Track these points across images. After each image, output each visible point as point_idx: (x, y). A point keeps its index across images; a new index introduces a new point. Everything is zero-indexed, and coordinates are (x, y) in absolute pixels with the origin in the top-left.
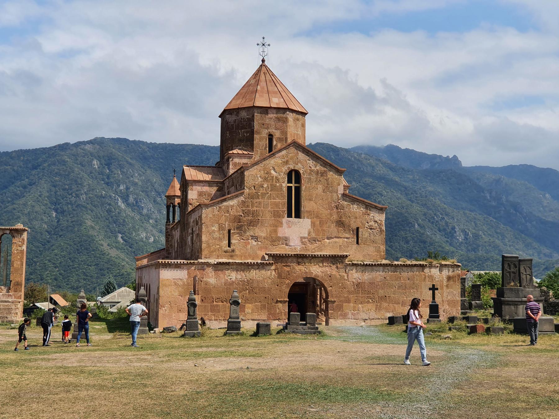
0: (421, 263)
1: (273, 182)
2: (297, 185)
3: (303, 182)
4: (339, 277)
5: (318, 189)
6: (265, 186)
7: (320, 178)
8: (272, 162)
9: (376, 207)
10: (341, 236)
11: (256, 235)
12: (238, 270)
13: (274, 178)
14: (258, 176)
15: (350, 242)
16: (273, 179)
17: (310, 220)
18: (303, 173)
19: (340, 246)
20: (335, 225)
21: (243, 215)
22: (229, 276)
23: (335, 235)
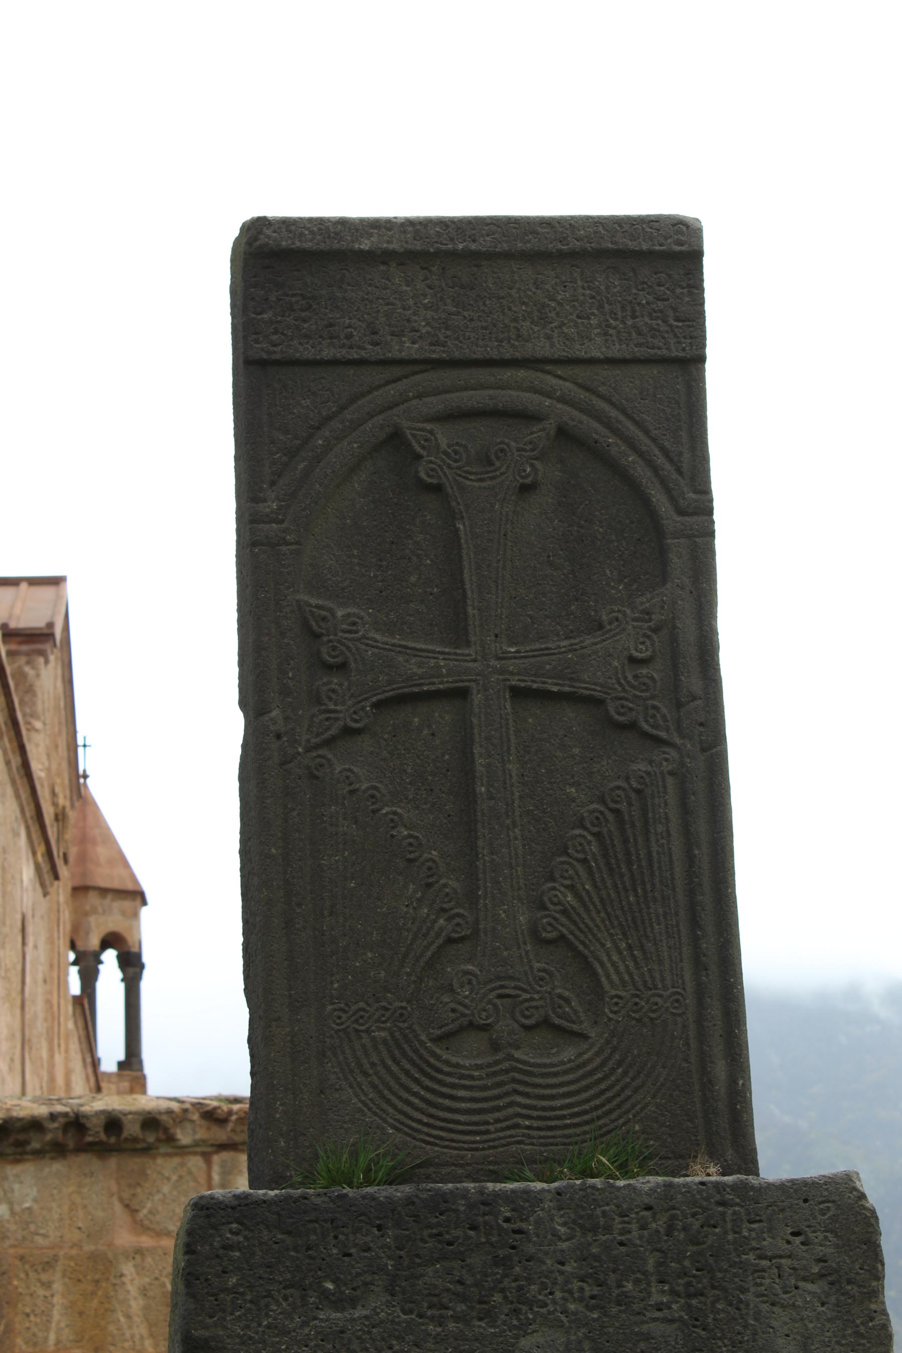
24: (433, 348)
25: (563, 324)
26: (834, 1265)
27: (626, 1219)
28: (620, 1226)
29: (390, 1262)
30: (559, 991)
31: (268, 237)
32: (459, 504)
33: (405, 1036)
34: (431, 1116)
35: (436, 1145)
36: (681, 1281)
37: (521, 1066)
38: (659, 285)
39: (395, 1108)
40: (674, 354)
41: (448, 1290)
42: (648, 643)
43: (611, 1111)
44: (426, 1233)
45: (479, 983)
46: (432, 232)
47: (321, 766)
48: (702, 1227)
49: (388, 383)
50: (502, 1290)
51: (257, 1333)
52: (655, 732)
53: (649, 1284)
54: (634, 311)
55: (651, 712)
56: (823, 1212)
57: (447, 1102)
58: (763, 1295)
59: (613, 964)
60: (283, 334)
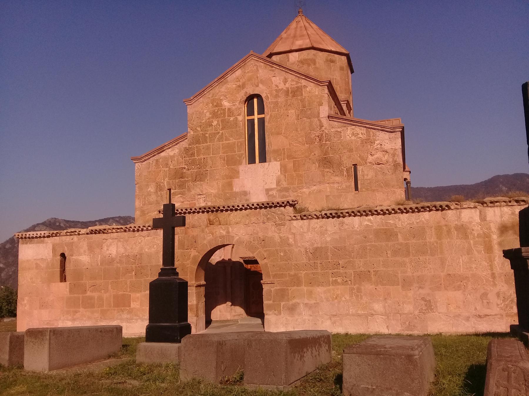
0: (438, 203)
1: (224, 116)
3: (266, 110)
6: (215, 123)
8: (223, 89)
9: (383, 129)
11: (204, 193)
12: (119, 241)
13: (227, 110)
14: (205, 111)
16: (224, 114)
18: (267, 97)
19: (327, 196)
20: (317, 165)
21: (186, 167)
22: (108, 249)
23: (318, 180)
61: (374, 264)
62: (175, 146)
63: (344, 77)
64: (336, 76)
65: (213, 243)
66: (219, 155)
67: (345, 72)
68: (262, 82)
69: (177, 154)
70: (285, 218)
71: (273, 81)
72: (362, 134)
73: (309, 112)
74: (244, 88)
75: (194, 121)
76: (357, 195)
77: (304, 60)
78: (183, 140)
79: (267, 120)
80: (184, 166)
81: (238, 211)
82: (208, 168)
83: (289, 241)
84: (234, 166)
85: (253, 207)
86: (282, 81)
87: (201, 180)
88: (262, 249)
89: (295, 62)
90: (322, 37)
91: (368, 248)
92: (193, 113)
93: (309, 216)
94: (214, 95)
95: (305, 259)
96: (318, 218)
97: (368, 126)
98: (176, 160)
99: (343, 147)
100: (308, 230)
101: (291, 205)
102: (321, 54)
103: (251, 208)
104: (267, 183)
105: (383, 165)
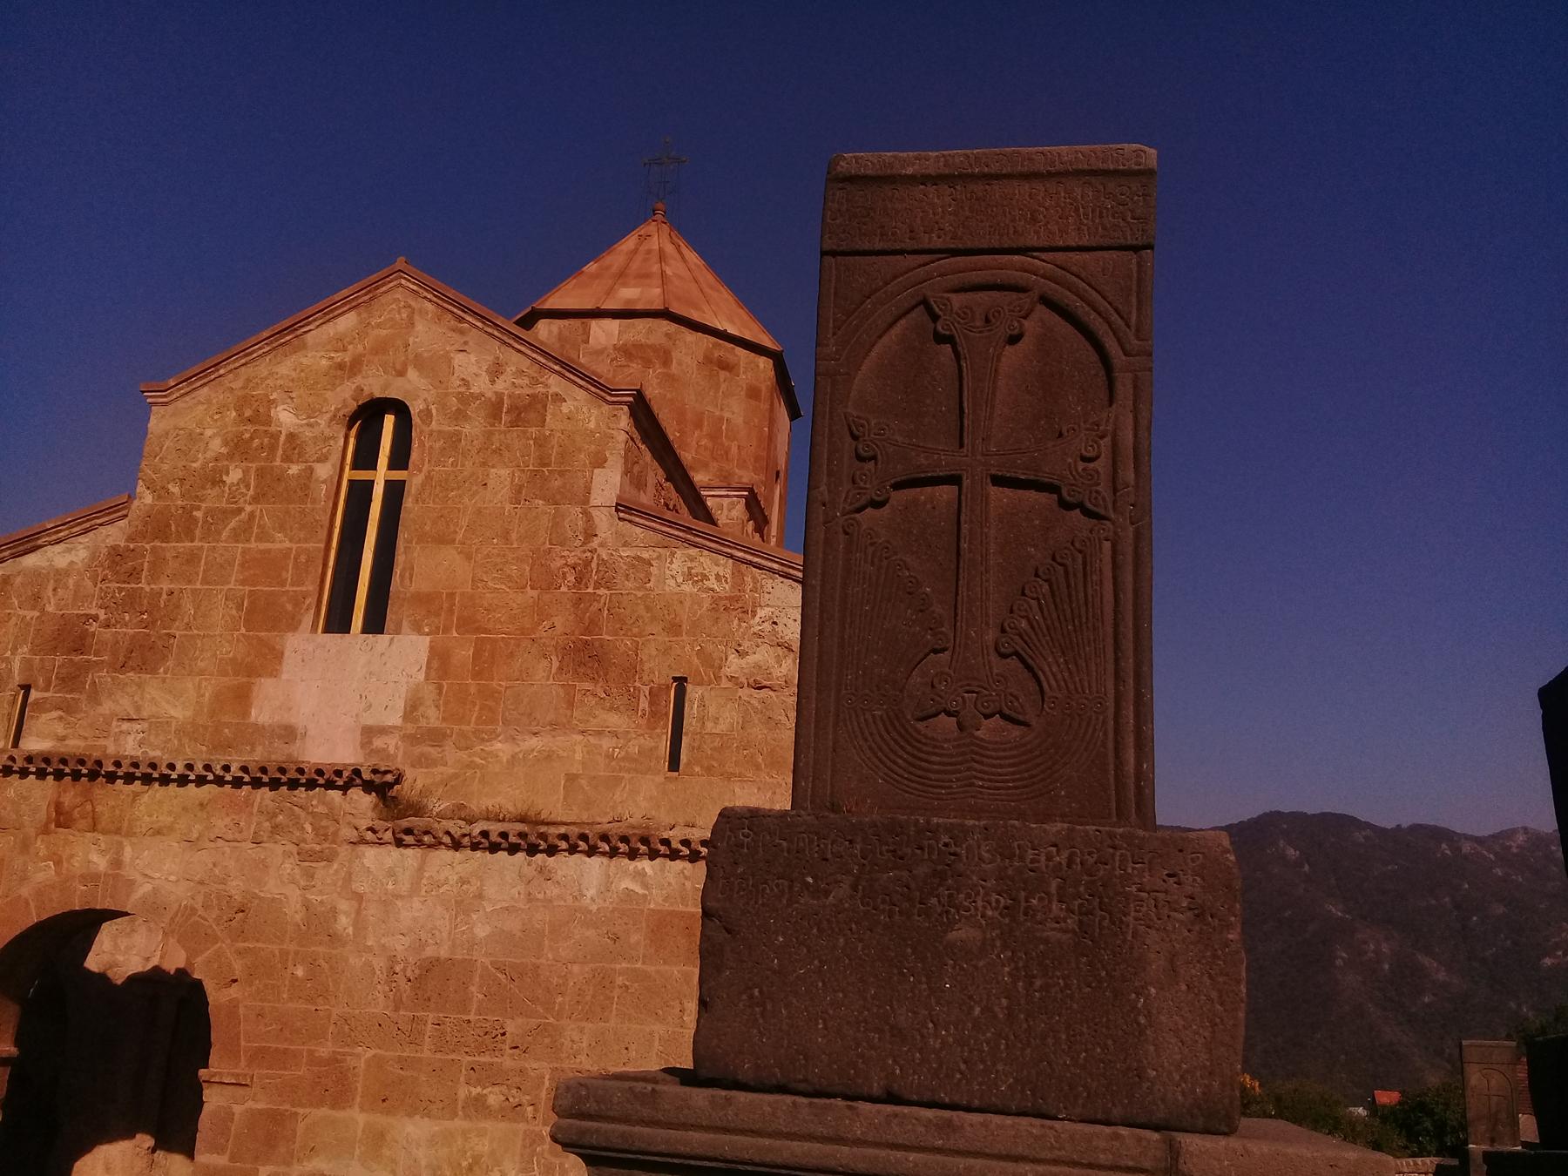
2: (398, 475)
3: (414, 456)
4: (298, 917)
5: (491, 484)
6: (234, 476)
7: (505, 433)
8: (286, 367)
10: (582, 727)
11: (145, 714)
13: (282, 438)
14: (209, 432)
15: (627, 758)
16: (273, 448)
17: (424, 642)
18: (427, 414)
19: (571, 778)
20: (556, 664)
21: (102, 616)
23: (551, 716)
24: (952, 241)
25: (1048, 222)
26: (1200, 902)
27: (1036, 852)
28: (1032, 857)
29: (857, 867)
30: (1009, 691)
31: (842, 167)
32: (963, 349)
33: (896, 715)
34: (910, 773)
35: (912, 793)
36: (1076, 903)
37: (978, 742)
38: (1122, 194)
39: (886, 766)
40: (1130, 242)
41: (897, 892)
42: (1095, 446)
43: (1043, 780)
44: (885, 848)
45: (952, 682)
46: (957, 161)
47: (852, 525)
48: (1096, 863)
49: (920, 266)
50: (937, 896)
51: (754, 908)
52: (1095, 509)
53: (1050, 902)
54: (1101, 213)
55: (1094, 495)
56: (1193, 860)
57: (923, 764)
58: (1141, 919)
59: (1053, 674)
60: (849, 233)
61: (632, 1047)
62: (80, 539)
63: (756, 420)
64: (733, 413)
65: (51, 900)
66: (226, 587)
67: (765, 406)
68: (419, 363)
69: (80, 564)
70: (335, 833)
71: (456, 367)
72: (717, 575)
73: (557, 483)
74: (355, 375)
75: (165, 461)
76: (672, 786)
77: (633, 345)
78: (112, 522)
79: (413, 491)
80: (93, 612)
81: (173, 786)
82: (178, 629)
83: (336, 920)
84: (267, 630)
85: (228, 778)
86: (484, 368)
87: (140, 669)
88: (228, 941)
89: (606, 348)
90: (707, 290)
91: (619, 980)
92: (167, 434)
93: (427, 833)
94: (251, 385)
95: (381, 997)
96: (456, 845)
97: (740, 554)
98: (71, 587)
99: (649, 615)
100: (415, 889)
101: (368, 787)
102: (690, 337)
103: (219, 781)
104: (370, 706)
105: (771, 693)
